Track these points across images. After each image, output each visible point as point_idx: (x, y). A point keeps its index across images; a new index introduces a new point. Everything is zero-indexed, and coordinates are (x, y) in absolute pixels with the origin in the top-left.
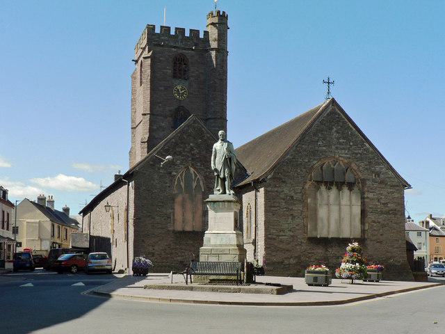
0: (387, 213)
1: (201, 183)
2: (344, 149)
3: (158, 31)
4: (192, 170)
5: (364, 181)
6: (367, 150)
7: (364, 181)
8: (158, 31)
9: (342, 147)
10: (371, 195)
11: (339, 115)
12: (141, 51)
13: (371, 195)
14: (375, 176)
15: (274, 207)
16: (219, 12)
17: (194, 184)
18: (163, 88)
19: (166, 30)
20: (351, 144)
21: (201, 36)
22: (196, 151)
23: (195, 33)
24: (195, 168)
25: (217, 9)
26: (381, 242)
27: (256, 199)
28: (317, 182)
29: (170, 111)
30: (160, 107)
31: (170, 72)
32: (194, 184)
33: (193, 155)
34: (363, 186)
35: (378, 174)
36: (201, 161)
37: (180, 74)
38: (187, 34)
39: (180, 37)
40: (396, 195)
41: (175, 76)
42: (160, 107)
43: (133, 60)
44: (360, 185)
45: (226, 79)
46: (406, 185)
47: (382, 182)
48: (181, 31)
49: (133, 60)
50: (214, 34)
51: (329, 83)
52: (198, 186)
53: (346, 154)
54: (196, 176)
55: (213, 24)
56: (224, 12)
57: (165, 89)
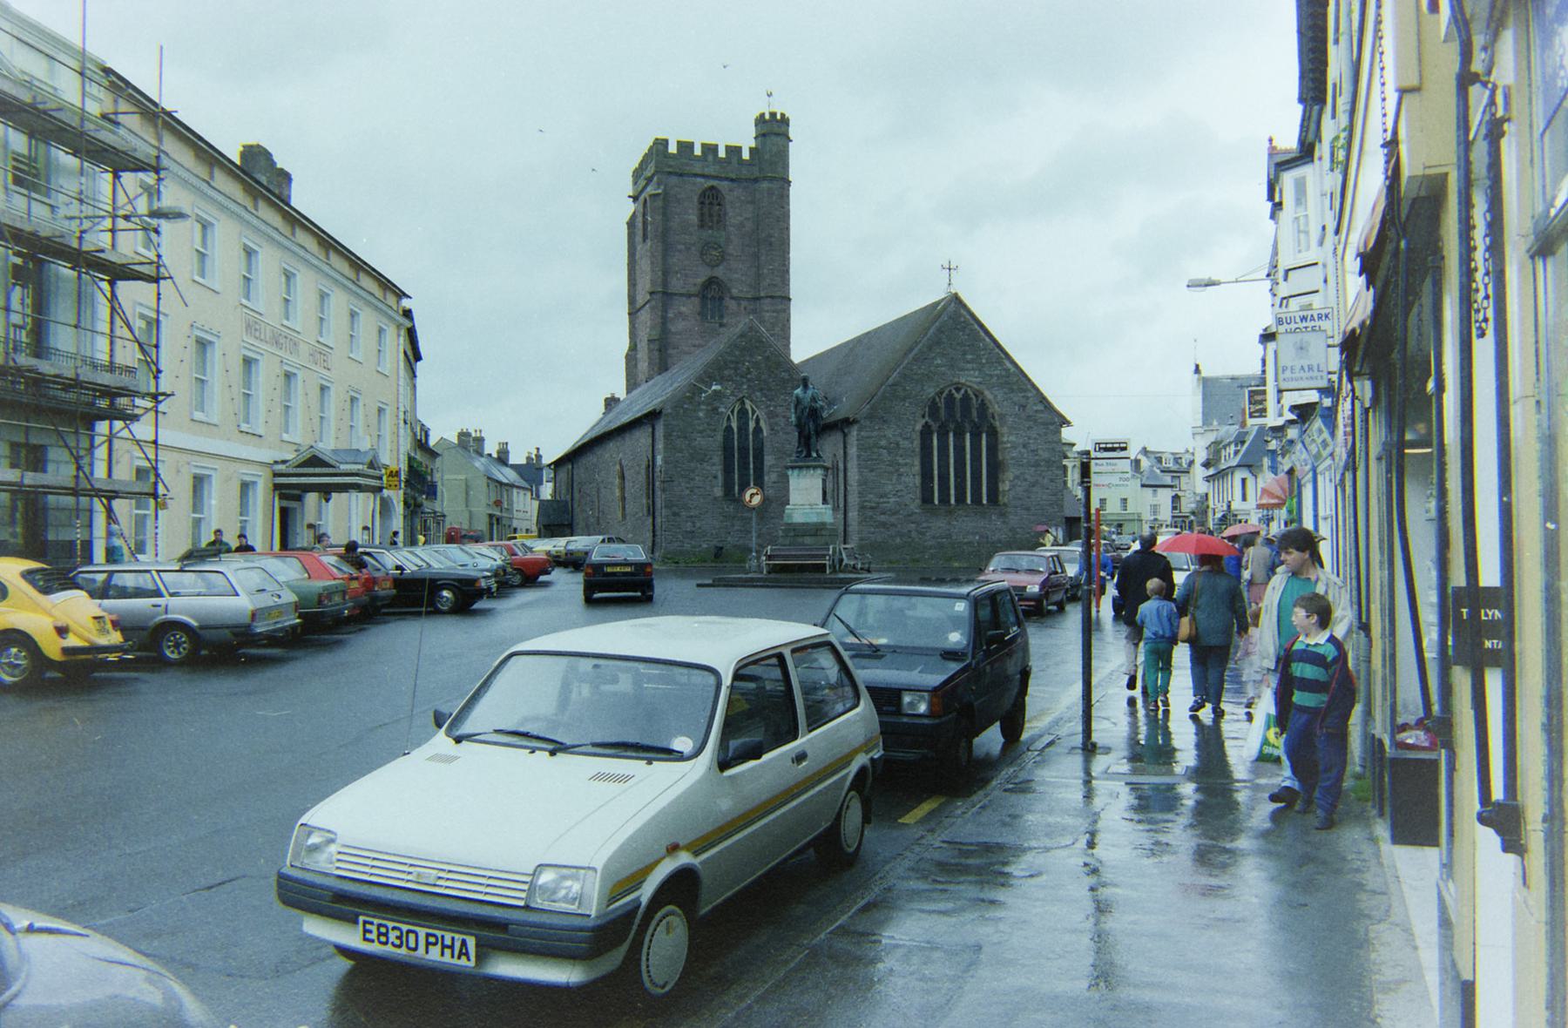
1: (762, 424)
2: (973, 369)
3: (673, 149)
5: (1002, 416)
6: (1007, 370)
7: (1002, 416)
8: (673, 149)
9: (969, 366)
12: (642, 183)
13: (1012, 438)
15: (872, 460)
16: (773, 115)
17: (752, 425)
18: (683, 247)
19: (686, 147)
20: (984, 361)
21: (746, 155)
23: (734, 151)
25: (772, 110)
26: (1028, 509)
27: (845, 447)
29: (695, 285)
30: (678, 279)
31: (693, 218)
32: (752, 425)
33: (749, 380)
37: (712, 221)
38: (722, 154)
39: (710, 158)
42: (678, 279)
43: (630, 197)
46: (1065, 422)
48: (710, 149)
49: (630, 197)
51: (950, 269)
52: (758, 430)
55: (764, 135)
56: (783, 115)
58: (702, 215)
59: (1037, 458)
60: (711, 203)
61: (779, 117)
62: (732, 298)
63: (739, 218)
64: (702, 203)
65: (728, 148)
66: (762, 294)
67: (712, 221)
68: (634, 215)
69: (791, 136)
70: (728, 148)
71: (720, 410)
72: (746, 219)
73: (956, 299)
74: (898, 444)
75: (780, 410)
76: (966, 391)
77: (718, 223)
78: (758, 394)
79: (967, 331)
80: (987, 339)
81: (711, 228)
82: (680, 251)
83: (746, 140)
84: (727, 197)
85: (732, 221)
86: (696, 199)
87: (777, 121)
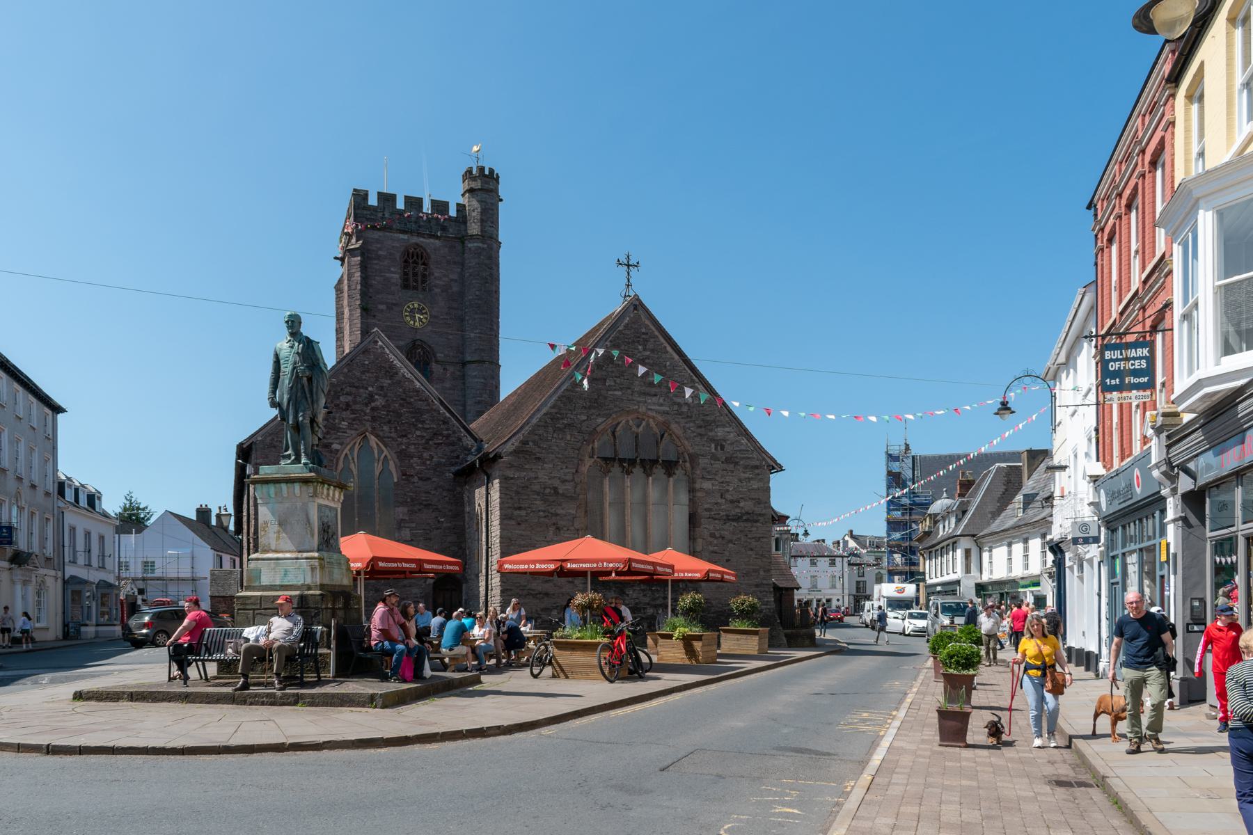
0: (737, 519)
3: (373, 201)
4: (373, 440)
5: (693, 458)
7: (693, 458)
8: (373, 201)
10: (707, 485)
11: (647, 327)
13: (707, 485)
14: (716, 449)
21: (453, 212)
22: (379, 401)
23: (440, 206)
24: (377, 436)
28: (605, 459)
31: (396, 277)
32: (378, 468)
34: (693, 468)
35: (720, 445)
36: (389, 422)
40: (755, 485)
41: (406, 286)
43: (336, 258)
44: (688, 465)
45: (497, 292)
46: (775, 467)
47: (727, 461)
49: (336, 258)
50: (473, 205)
53: (661, 405)
54: (381, 452)
57: (387, 307)
58: (406, 274)
59: (738, 510)
60: (415, 262)
61: (487, 172)
62: (437, 362)
63: (444, 279)
64: (406, 261)
65: (434, 203)
66: (469, 359)
67: (416, 281)
68: (340, 281)
69: (502, 193)
70: (434, 203)
71: (336, 446)
72: (452, 280)
73: (636, 306)
74: (555, 489)
75: (412, 449)
76: (648, 425)
77: (424, 282)
78: (386, 428)
79: (650, 346)
80: (676, 357)
81: (415, 288)
82: (382, 310)
83: (454, 194)
84: (433, 256)
85: (438, 282)
86: (398, 256)
87: (486, 176)
